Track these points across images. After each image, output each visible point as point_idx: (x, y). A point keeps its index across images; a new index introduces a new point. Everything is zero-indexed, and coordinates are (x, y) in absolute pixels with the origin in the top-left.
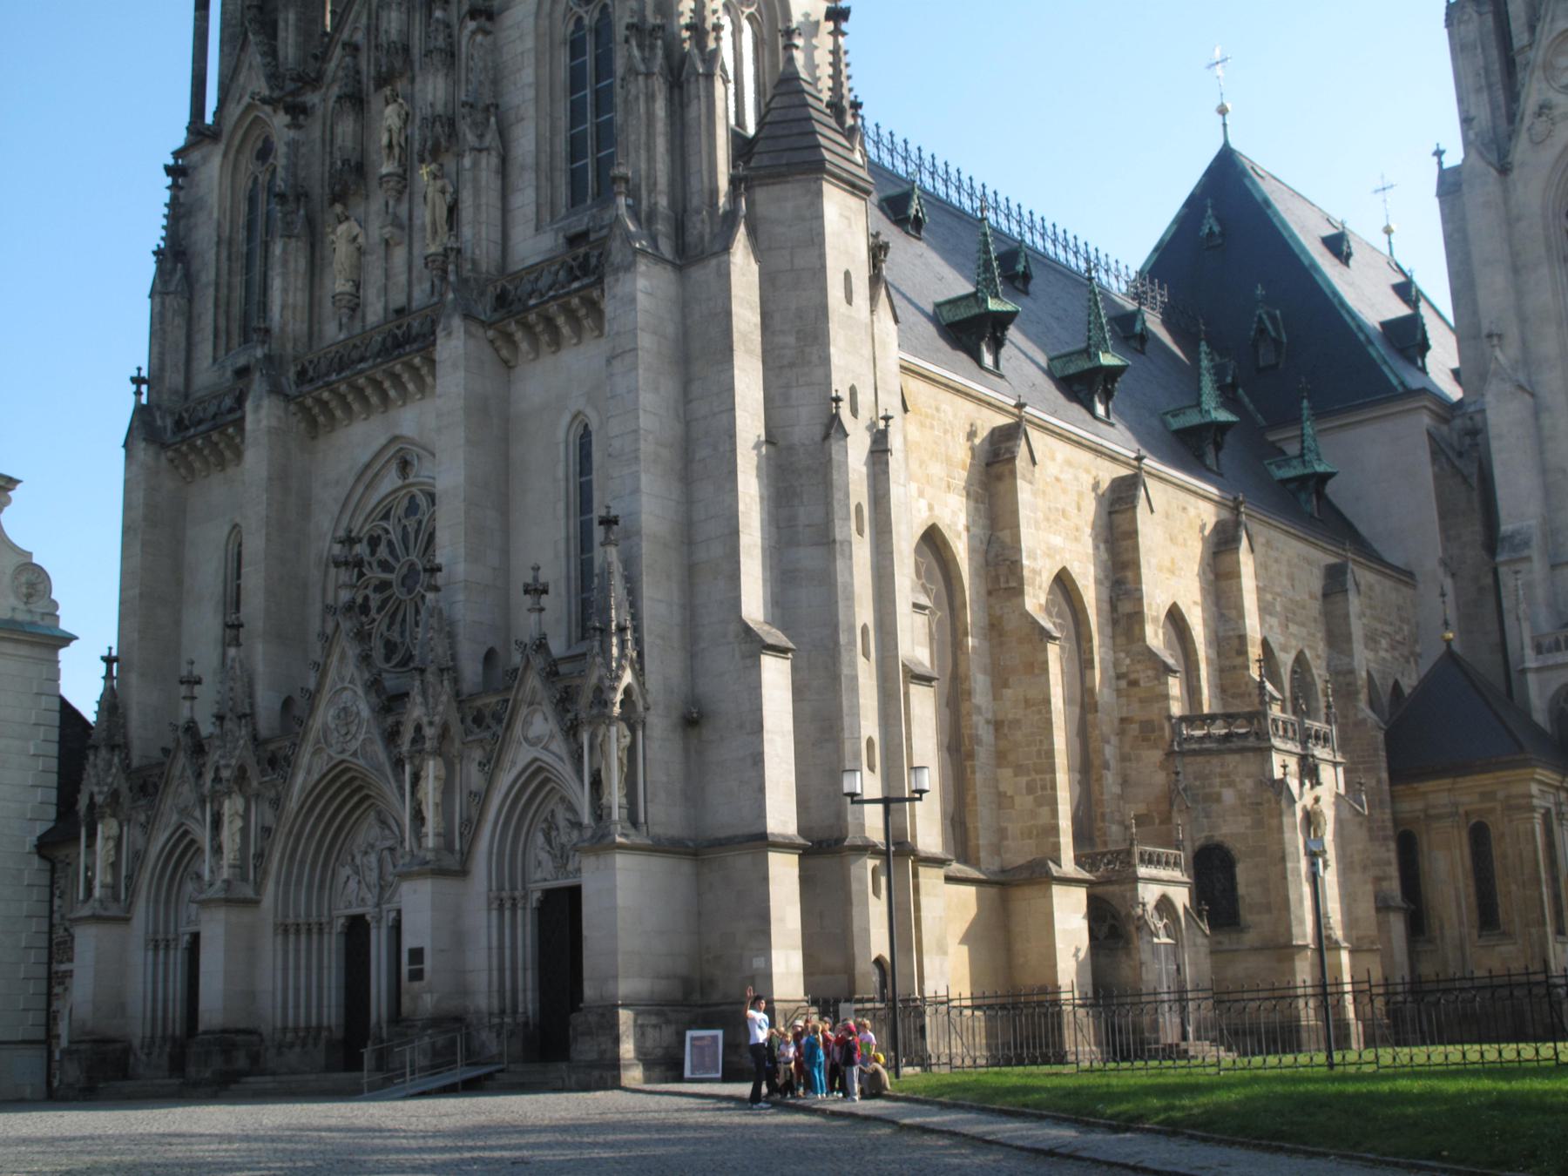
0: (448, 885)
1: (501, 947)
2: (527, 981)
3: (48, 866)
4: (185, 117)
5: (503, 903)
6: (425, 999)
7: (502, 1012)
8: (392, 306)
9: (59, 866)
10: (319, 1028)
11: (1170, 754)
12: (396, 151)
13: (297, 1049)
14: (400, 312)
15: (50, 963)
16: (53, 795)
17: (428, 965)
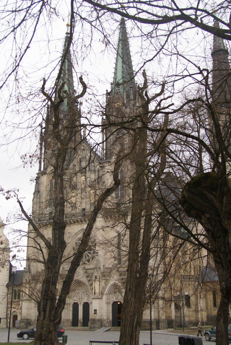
0: (100, 300)
1: (107, 310)
2: (111, 315)
3: (7, 289)
4: (38, 169)
5: (108, 303)
6: (97, 317)
7: (107, 319)
8: (82, 208)
9: (9, 289)
10: (69, 320)
11: (181, 281)
12: (84, 184)
13: (66, 323)
14: (84, 209)
15: (7, 305)
16: (8, 277)
17: (98, 312)
